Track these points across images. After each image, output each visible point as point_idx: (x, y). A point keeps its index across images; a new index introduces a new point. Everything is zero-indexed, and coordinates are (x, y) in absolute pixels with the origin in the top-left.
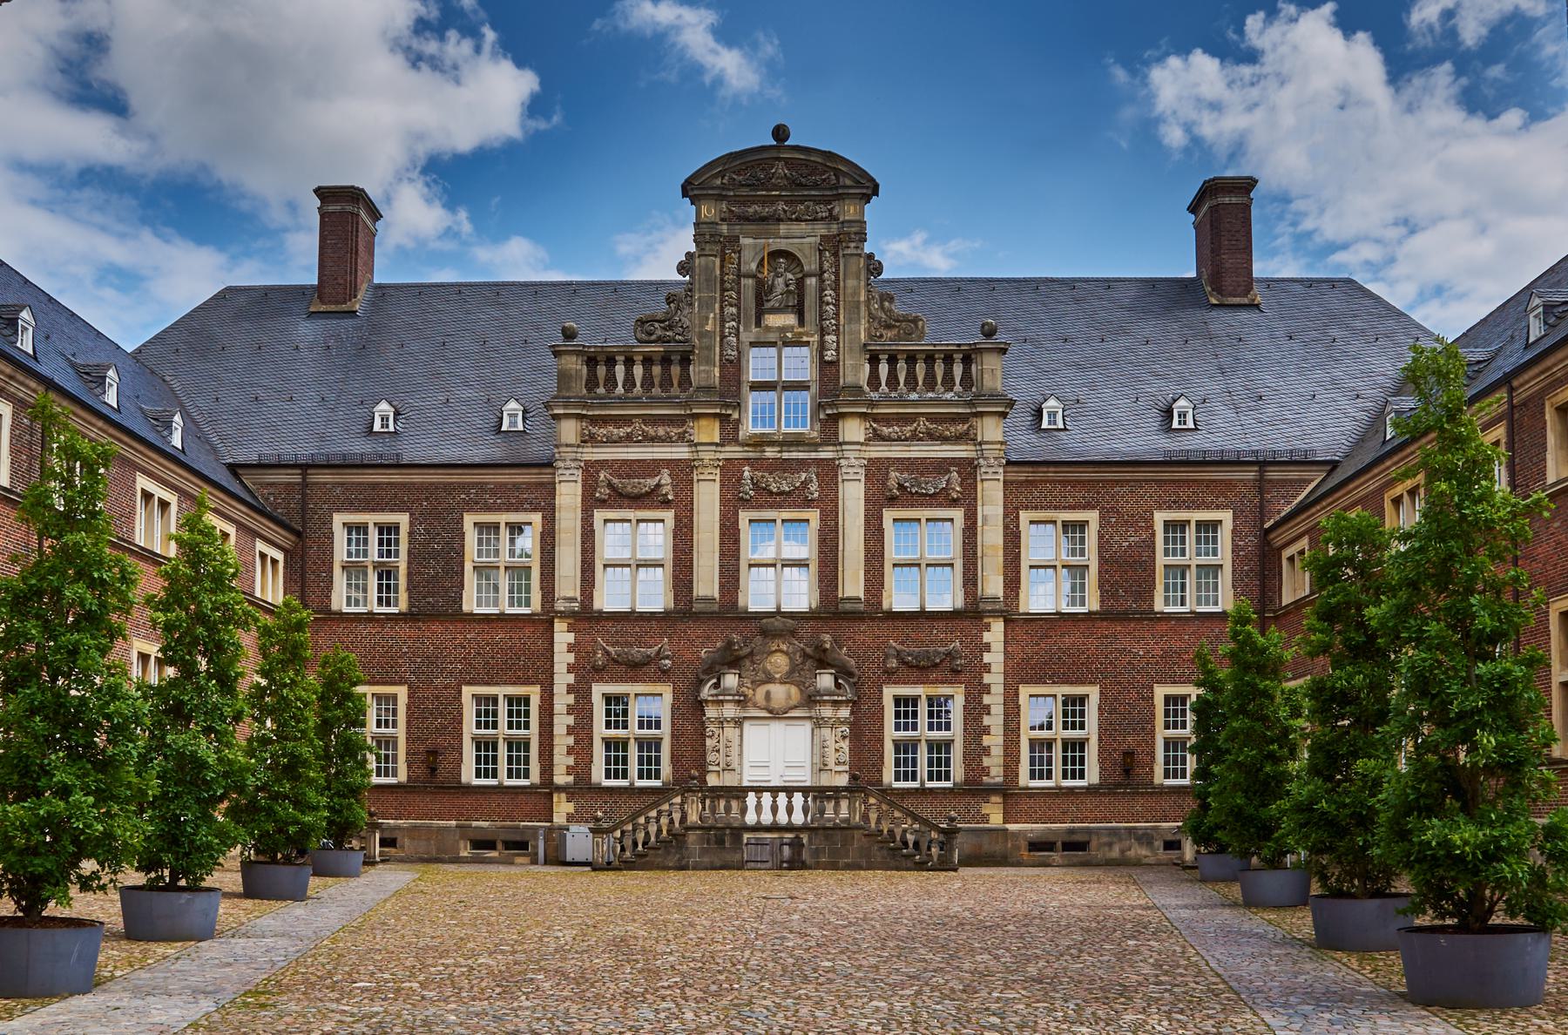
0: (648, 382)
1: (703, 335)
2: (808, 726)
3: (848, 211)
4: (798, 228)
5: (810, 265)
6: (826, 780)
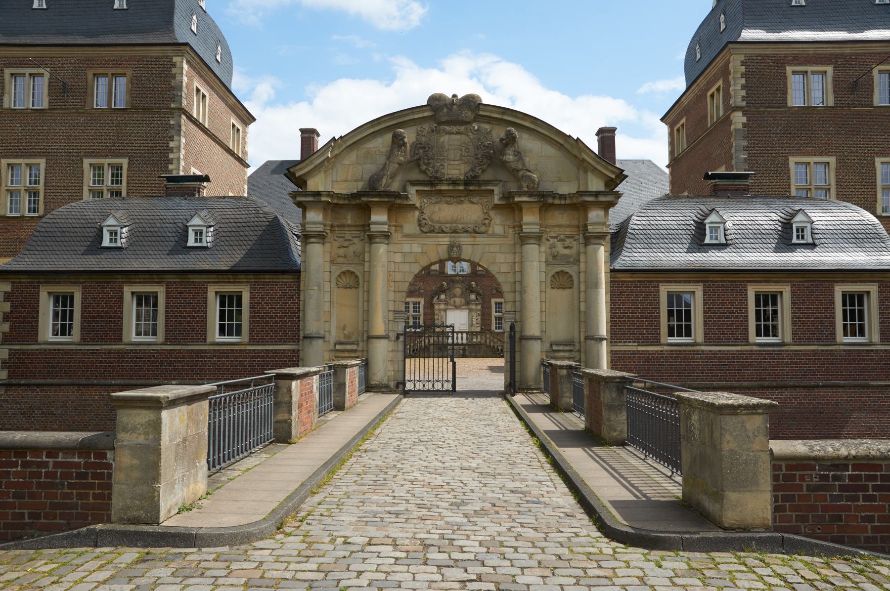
6: (473, 329)
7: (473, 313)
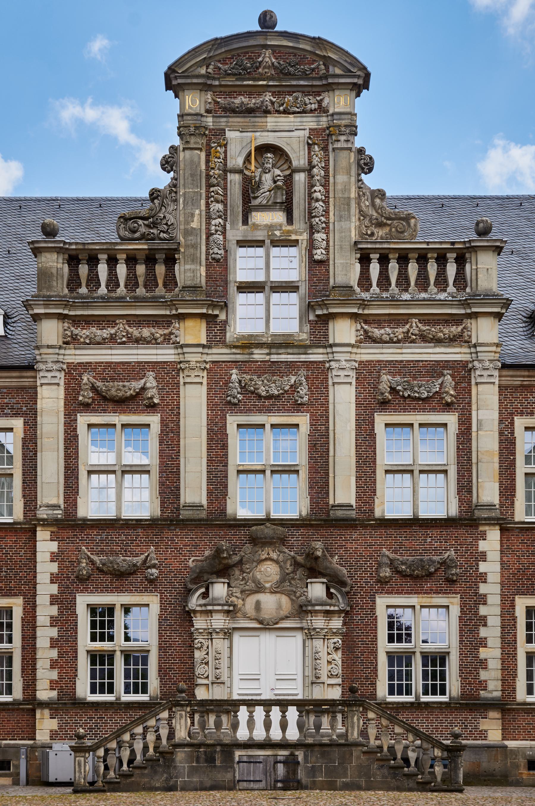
0: (132, 281)
1: (188, 232)
3: (338, 102)
4: (289, 121)
5: (299, 159)
6: (318, 693)
7: (318, 644)
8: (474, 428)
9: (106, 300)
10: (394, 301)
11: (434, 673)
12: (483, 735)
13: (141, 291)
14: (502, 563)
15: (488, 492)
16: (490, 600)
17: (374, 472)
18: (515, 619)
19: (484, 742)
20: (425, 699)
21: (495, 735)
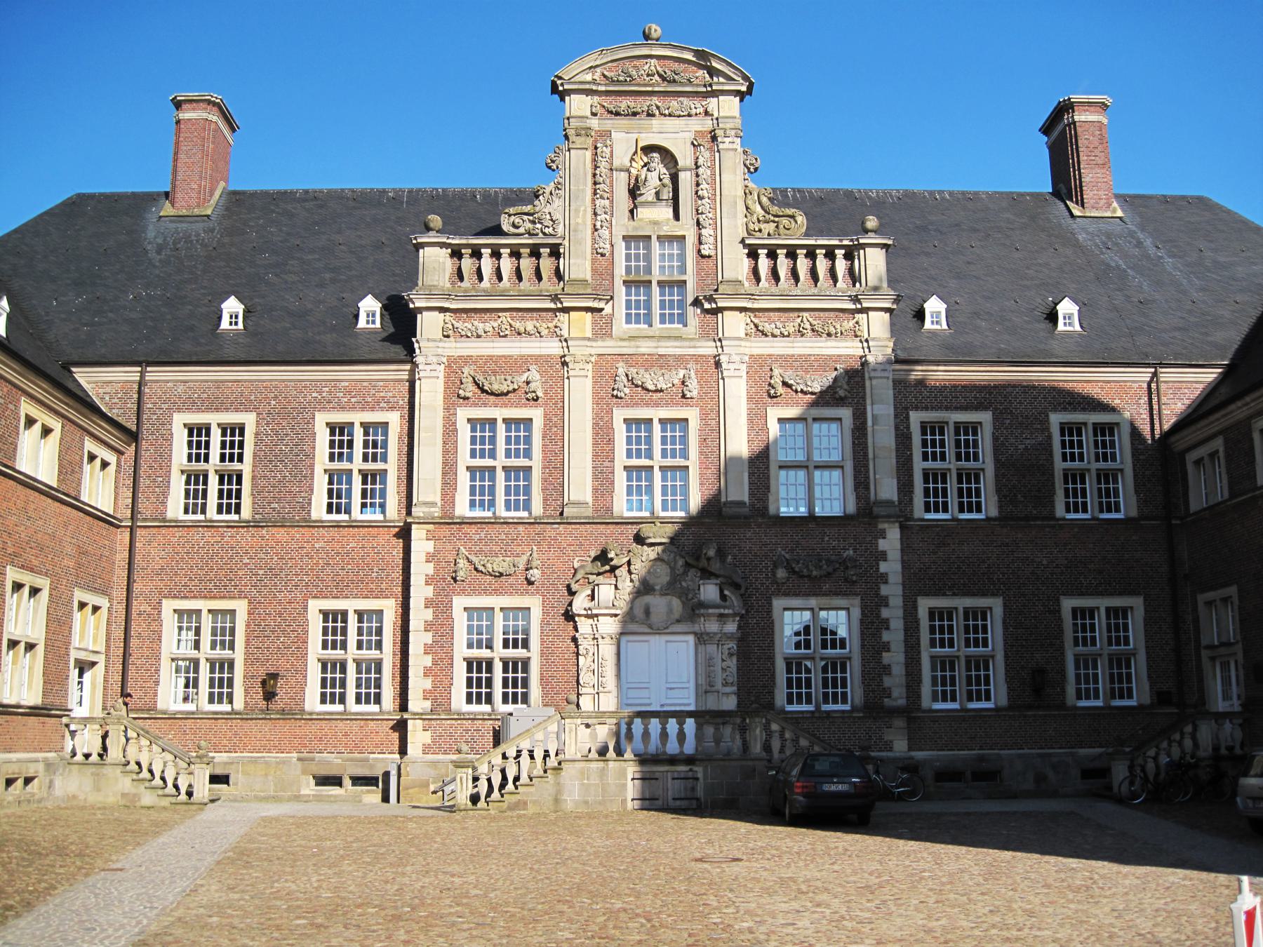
2: (691, 639)
5: (684, 157)
6: (712, 704)
7: (712, 649)
8: (870, 423)
9: (489, 295)
10: (784, 296)
11: (835, 679)
12: (889, 746)
13: (525, 285)
14: (903, 562)
15: (886, 489)
16: (892, 602)
17: (768, 468)
18: (917, 621)
19: (890, 754)
20: (825, 707)
21: (900, 746)
